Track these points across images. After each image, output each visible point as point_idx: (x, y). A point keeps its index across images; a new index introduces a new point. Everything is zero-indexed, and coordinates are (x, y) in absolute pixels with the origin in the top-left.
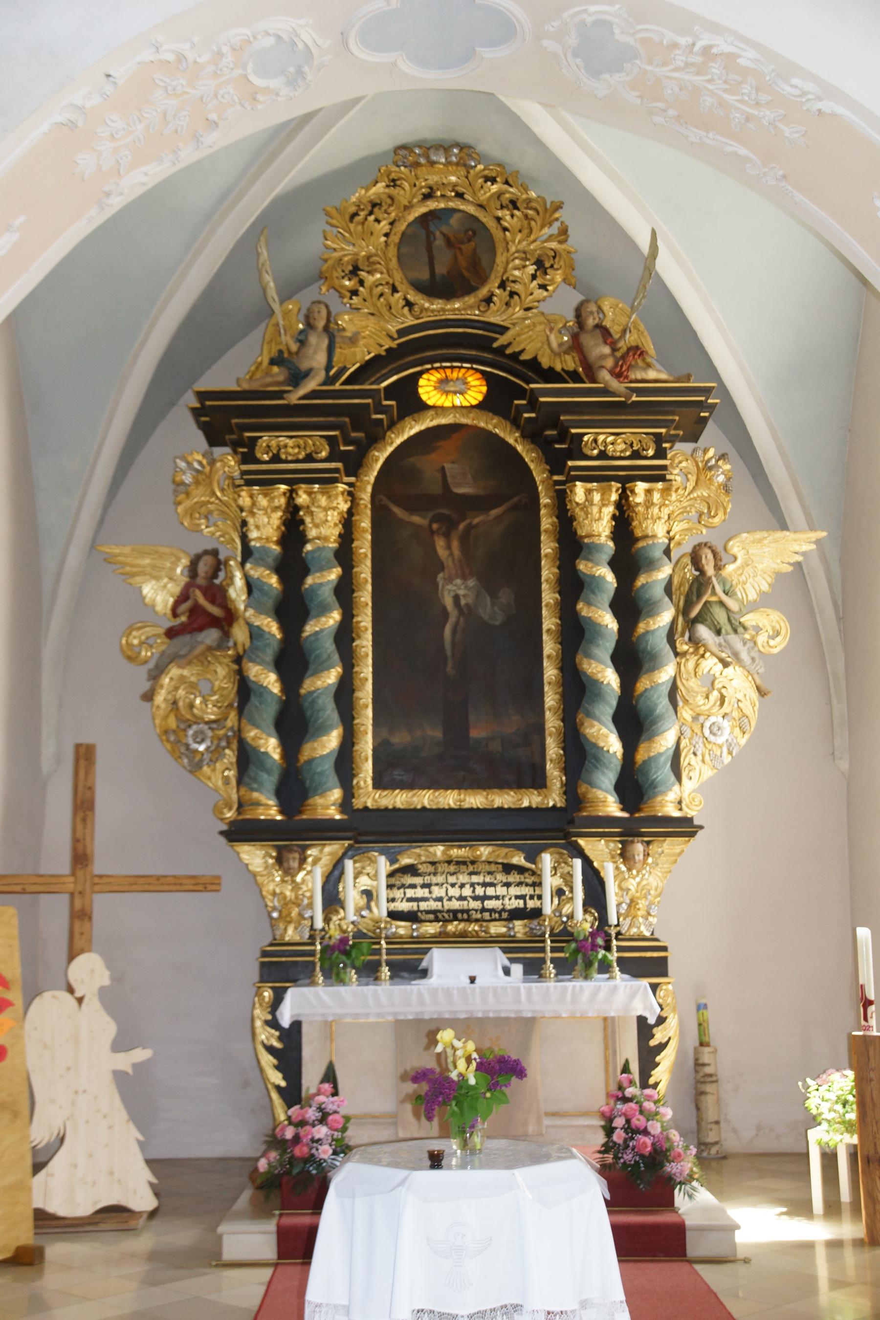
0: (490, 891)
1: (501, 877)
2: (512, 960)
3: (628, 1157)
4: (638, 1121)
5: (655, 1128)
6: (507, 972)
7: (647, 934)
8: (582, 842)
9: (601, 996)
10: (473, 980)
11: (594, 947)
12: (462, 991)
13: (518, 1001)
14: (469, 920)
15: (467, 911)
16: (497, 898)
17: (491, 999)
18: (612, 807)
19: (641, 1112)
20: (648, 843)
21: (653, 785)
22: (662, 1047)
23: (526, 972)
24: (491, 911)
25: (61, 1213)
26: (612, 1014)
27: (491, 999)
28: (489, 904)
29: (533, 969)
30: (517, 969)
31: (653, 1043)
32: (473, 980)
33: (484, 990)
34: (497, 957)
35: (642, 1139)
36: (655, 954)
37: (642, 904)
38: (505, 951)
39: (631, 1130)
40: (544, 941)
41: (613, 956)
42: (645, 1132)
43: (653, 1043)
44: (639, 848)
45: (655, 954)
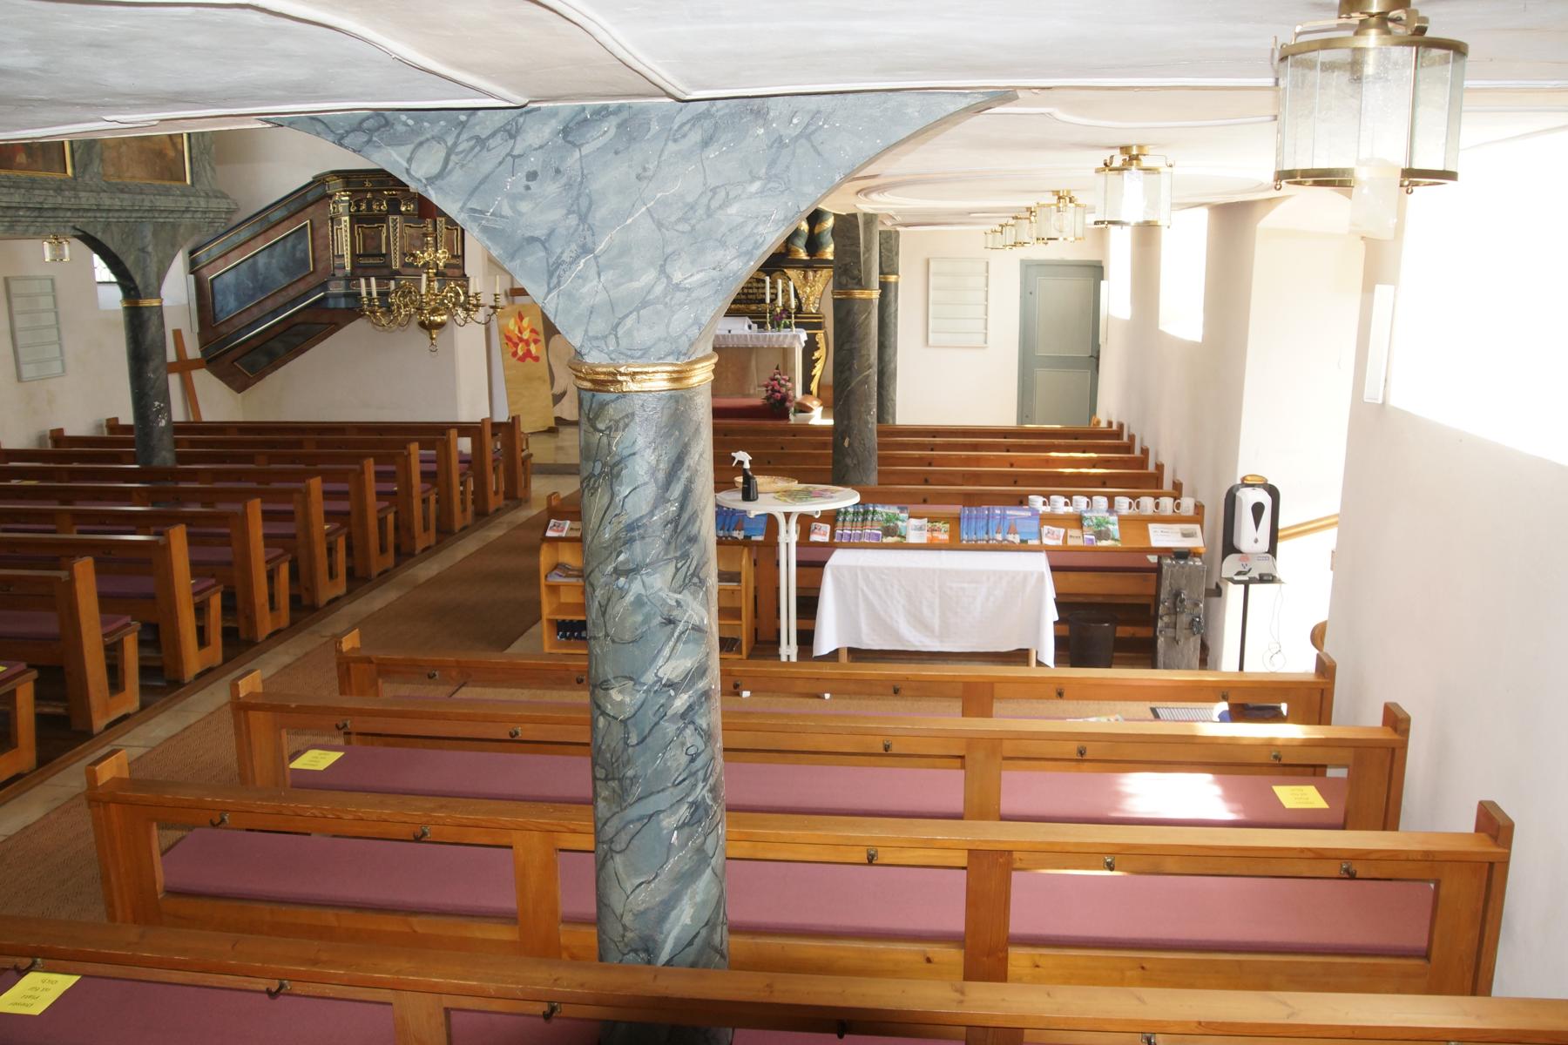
0: (751, 291)
1: (755, 285)
2: (753, 322)
3: (772, 401)
4: (777, 388)
5: (783, 390)
6: (750, 327)
7: (814, 311)
8: (785, 270)
9: (781, 338)
10: (730, 331)
11: (781, 318)
12: (724, 336)
13: (746, 340)
14: (741, 304)
15: (740, 300)
16: (753, 294)
17: (735, 339)
18: (803, 255)
19: (779, 384)
20: (815, 271)
21: (821, 244)
22: (818, 359)
23: (759, 328)
24: (751, 299)
25: (568, 418)
26: (785, 346)
27: (735, 339)
28: (750, 297)
29: (762, 326)
30: (755, 326)
31: (814, 358)
32: (730, 331)
33: (733, 336)
34: (747, 321)
35: (777, 394)
36: (816, 320)
37: (812, 298)
38: (750, 317)
39: (773, 391)
40: (765, 317)
41: (793, 321)
42: (779, 392)
43: (814, 358)
44: (811, 274)
45: (816, 320)
